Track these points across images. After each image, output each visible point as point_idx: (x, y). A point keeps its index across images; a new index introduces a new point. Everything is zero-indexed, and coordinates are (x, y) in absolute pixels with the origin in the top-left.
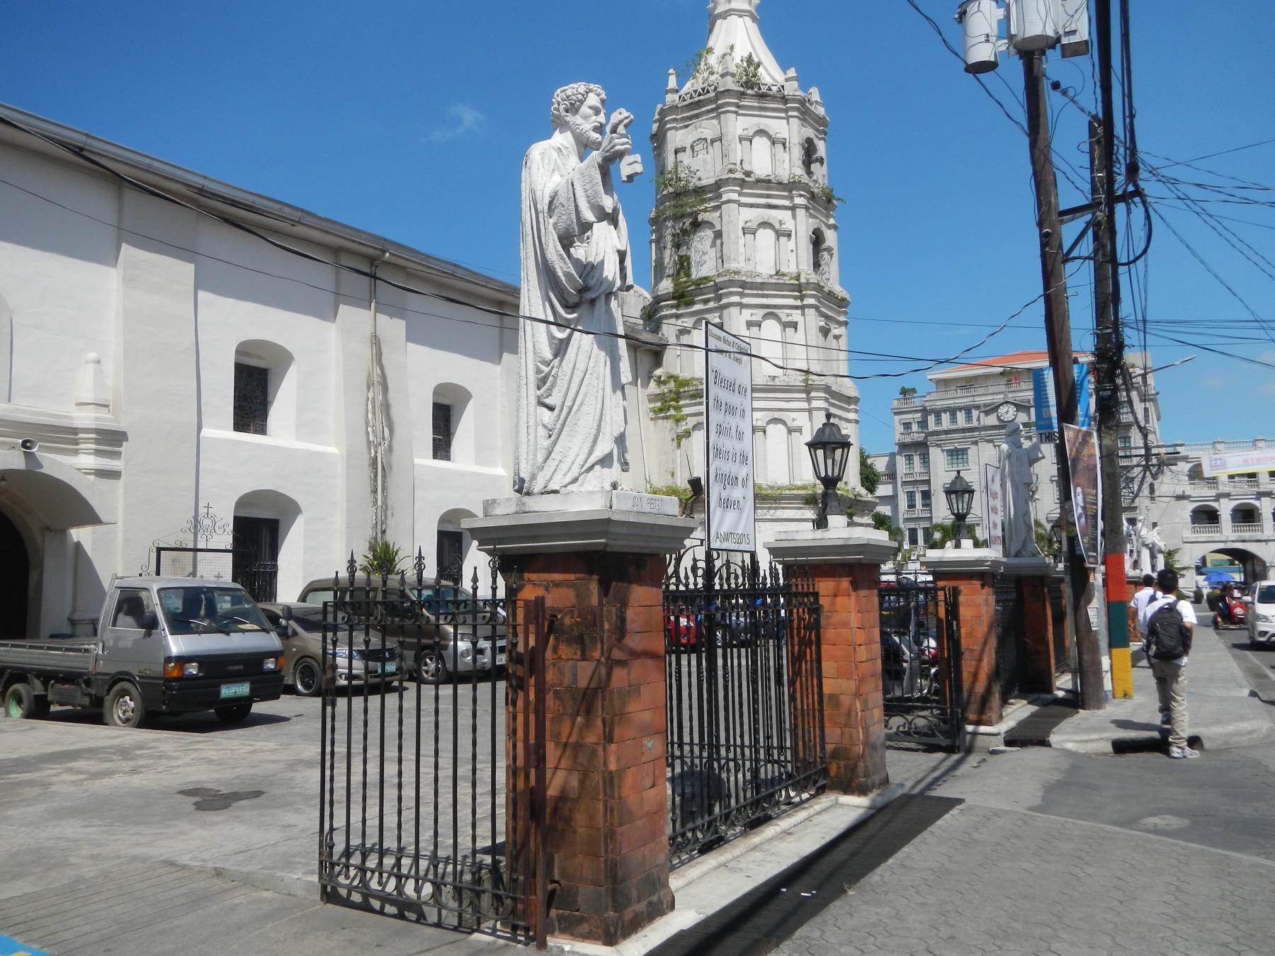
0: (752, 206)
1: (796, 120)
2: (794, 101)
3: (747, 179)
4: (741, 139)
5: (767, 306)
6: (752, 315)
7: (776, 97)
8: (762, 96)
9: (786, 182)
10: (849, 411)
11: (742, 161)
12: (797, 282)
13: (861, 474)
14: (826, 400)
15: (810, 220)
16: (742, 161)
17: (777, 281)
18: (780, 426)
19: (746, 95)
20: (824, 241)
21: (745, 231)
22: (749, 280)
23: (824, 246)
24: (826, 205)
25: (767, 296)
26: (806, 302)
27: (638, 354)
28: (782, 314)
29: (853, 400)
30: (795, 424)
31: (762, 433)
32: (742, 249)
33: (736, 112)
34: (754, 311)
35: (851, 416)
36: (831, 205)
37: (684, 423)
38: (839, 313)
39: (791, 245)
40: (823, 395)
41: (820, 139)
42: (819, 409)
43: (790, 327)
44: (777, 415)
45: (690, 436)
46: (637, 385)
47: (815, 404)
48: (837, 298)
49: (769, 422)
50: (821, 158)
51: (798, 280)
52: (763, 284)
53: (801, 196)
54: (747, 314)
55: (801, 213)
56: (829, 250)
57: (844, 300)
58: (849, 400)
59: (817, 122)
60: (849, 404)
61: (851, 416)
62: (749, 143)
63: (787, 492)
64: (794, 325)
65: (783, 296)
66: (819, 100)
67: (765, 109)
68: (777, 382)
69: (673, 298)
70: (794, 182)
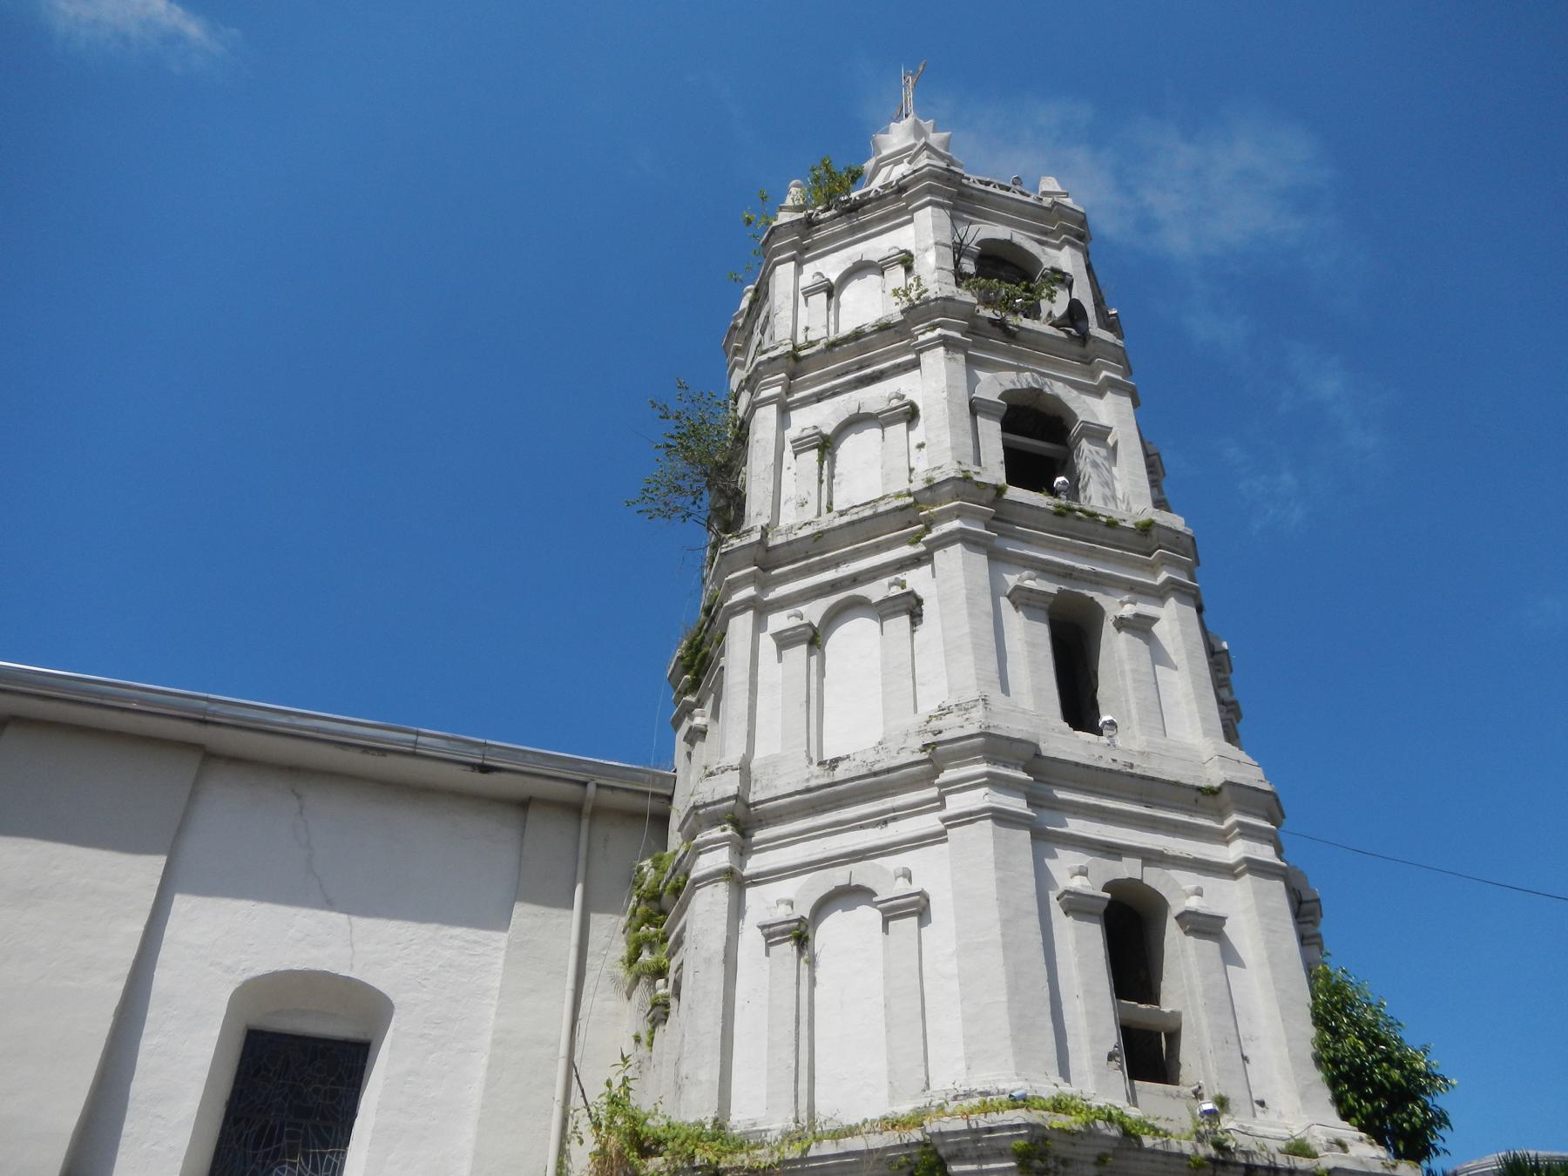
0: (819, 398)
1: (929, 209)
2: (918, 180)
3: (803, 353)
4: (809, 293)
5: (834, 586)
6: (789, 617)
7: (885, 196)
8: (855, 208)
9: (900, 318)
10: (1223, 838)
11: (807, 329)
12: (911, 500)
13: (1318, 1061)
14: (994, 782)
15: (983, 375)
16: (807, 329)
17: (855, 517)
18: (868, 915)
19: (820, 222)
20: (1074, 416)
21: (800, 447)
22: (779, 540)
23: (1075, 431)
24: (1076, 349)
25: (836, 563)
26: (936, 532)
27: (585, 822)
28: (877, 591)
29: (1226, 794)
30: (901, 887)
31: (789, 948)
32: (789, 488)
33: (792, 258)
34: (803, 609)
35: (1235, 851)
36: (1090, 345)
37: (660, 982)
38: (1153, 569)
39: (917, 435)
40: (983, 768)
41: (1059, 248)
42: (968, 818)
43: (895, 614)
44: (838, 877)
45: (667, 1014)
46: (572, 908)
47: (958, 803)
48: (1112, 524)
49: (824, 905)
50: (1055, 271)
51: (910, 494)
52: (819, 536)
53: (934, 327)
54: (779, 621)
55: (935, 360)
56: (1099, 434)
57: (1146, 528)
58: (1208, 798)
59: (1035, 218)
60: (1220, 815)
61: (1235, 851)
62: (824, 295)
63: (828, 1148)
64: (912, 607)
65: (878, 548)
66: (1058, 189)
67: (863, 226)
68: (841, 773)
69: (687, 669)
70: (913, 307)
